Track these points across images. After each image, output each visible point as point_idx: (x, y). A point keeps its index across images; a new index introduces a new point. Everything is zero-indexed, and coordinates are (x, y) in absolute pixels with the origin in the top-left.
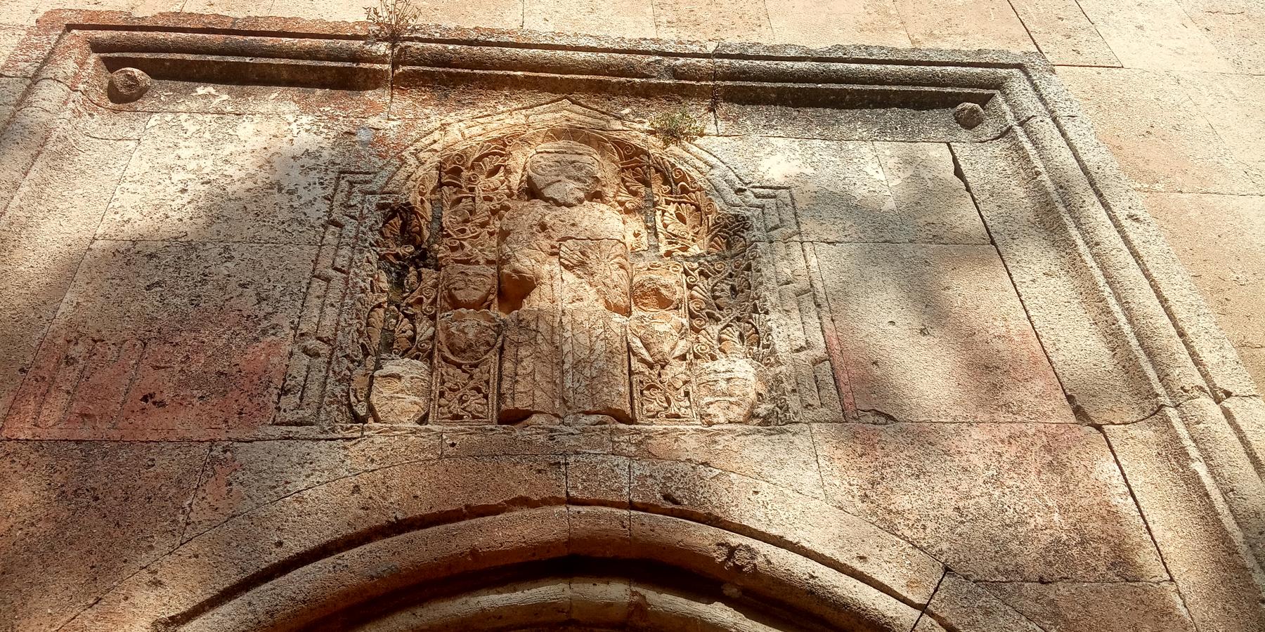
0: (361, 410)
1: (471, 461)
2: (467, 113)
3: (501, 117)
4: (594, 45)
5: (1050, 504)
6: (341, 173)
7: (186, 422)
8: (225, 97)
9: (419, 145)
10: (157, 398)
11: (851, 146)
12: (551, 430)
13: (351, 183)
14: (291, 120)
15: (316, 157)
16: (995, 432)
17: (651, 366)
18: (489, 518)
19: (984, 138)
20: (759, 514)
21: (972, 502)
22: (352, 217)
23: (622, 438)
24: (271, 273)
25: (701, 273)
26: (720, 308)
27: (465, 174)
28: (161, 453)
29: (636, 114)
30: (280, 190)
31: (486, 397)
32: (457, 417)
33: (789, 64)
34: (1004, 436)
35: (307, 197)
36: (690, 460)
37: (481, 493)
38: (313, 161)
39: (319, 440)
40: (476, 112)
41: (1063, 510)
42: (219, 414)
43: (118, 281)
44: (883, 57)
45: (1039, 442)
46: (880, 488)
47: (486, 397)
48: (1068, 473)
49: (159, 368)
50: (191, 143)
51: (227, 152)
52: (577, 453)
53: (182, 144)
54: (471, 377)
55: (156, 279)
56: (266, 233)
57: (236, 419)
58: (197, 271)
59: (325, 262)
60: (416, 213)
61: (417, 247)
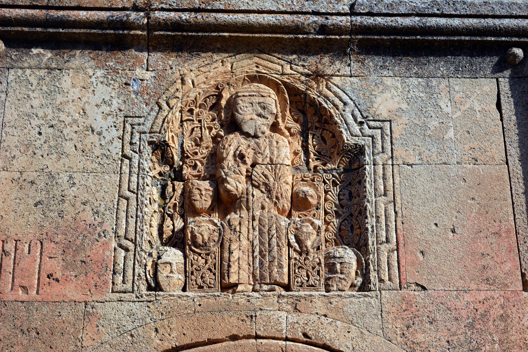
0: (153, 285)
1: (209, 314)
2: (196, 62)
3: (215, 65)
4: (274, 9)
5: (495, 339)
6: (125, 117)
7: (71, 291)
8: (49, 55)
9: (168, 94)
10: (54, 277)
11: (434, 82)
12: (248, 296)
13: (132, 125)
14: (91, 74)
15: (109, 105)
16: (477, 297)
17: (301, 255)
18: (219, 345)
19: (520, 75)
20: (349, 345)
21: (456, 337)
22: (136, 152)
23: (283, 301)
24: (97, 195)
25: (333, 181)
26: (342, 206)
27: (196, 110)
28: (62, 309)
29: (300, 59)
30: (93, 131)
31: (214, 274)
32: (201, 287)
33: (400, 20)
34: (481, 299)
35: (109, 138)
36: (317, 313)
37: (215, 332)
38: (108, 108)
39: (135, 302)
40: (200, 62)
41: (501, 342)
42: (86, 286)
43: (18, 201)
44: (463, 12)
45: (499, 303)
46: (411, 330)
47: (214, 274)
48: (509, 321)
49: (51, 258)
50: (35, 95)
51: (58, 102)
52: (261, 310)
53: (32, 95)
54: (206, 263)
55: (38, 199)
56: (91, 166)
57: (94, 289)
58: (58, 193)
59: (125, 186)
60: (169, 146)
61: (171, 167)
